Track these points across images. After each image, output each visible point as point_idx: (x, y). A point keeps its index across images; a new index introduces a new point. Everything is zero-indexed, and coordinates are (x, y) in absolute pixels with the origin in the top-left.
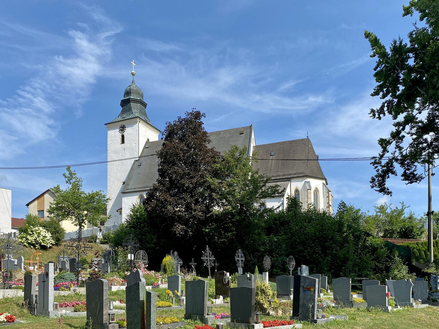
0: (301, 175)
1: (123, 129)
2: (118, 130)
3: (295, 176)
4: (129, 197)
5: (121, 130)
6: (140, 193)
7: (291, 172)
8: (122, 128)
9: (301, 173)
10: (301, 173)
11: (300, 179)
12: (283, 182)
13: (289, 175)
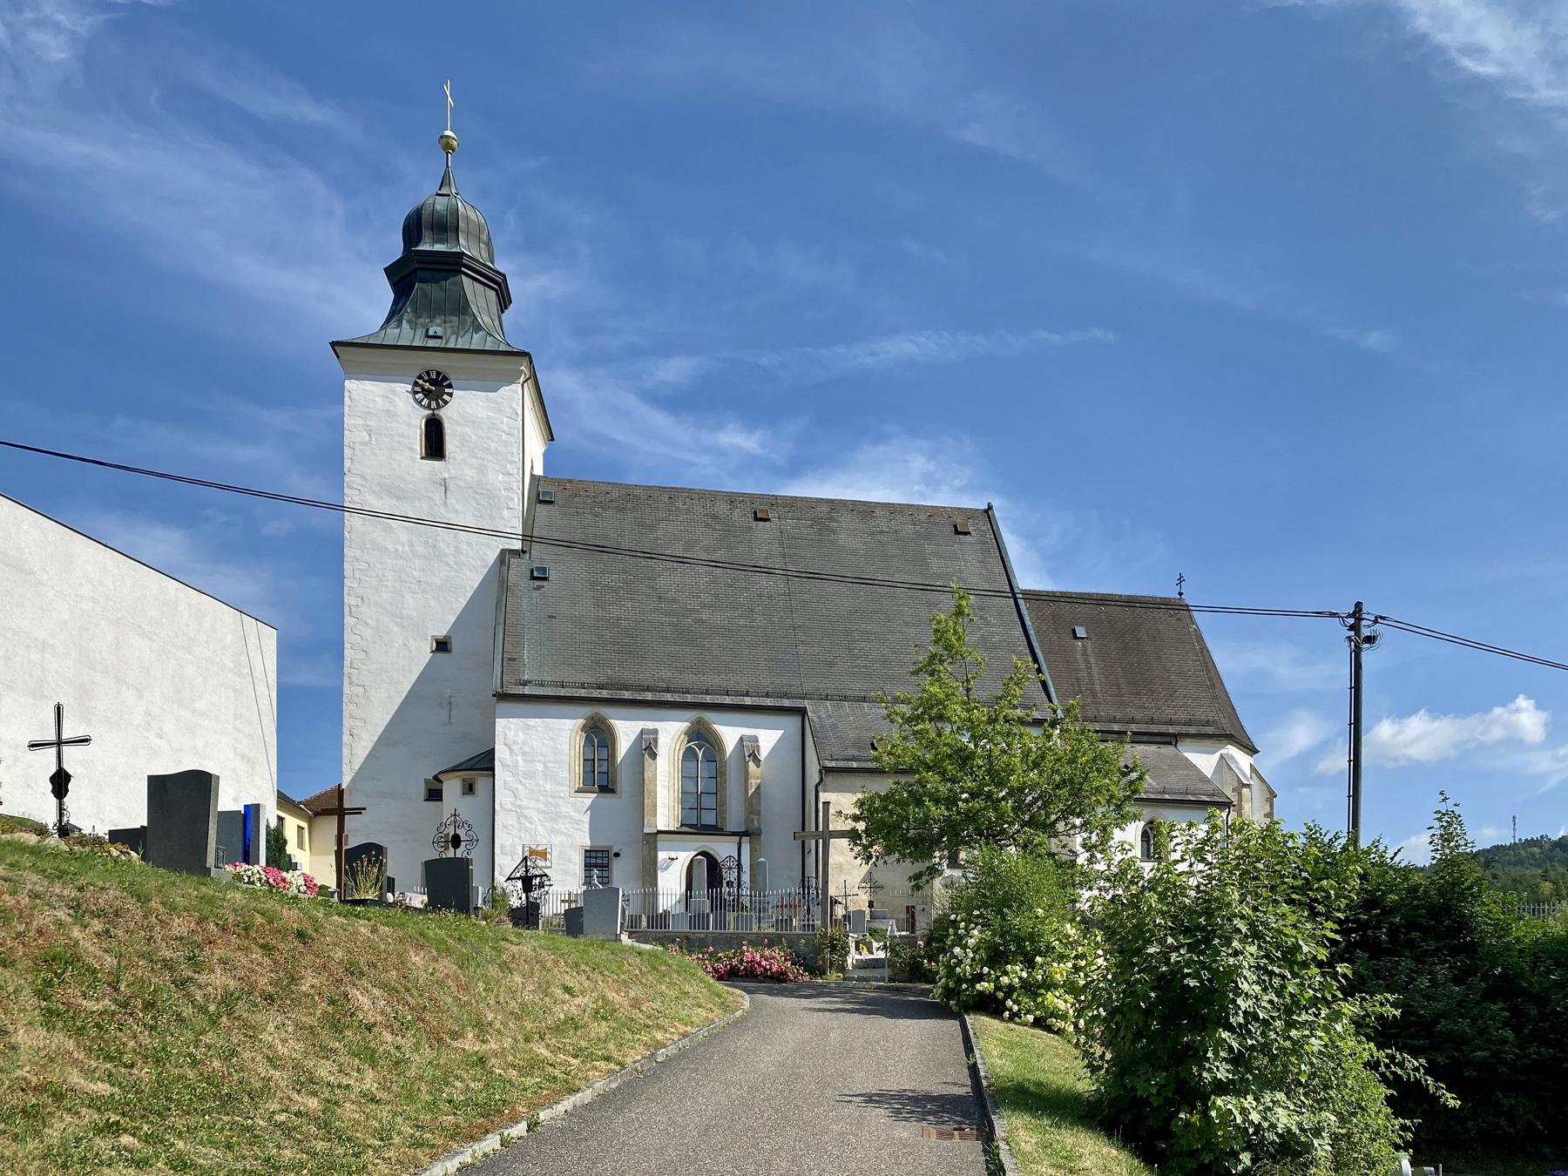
0: (1210, 730)
1: (434, 388)
2: (409, 387)
3: (1192, 730)
4: (532, 722)
5: (427, 393)
6: (588, 710)
7: (1169, 712)
8: (432, 382)
9: (1208, 723)
10: (1208, 723)
11: (1207, 742)
12: (1154, 747)
13: (1170, 723)
